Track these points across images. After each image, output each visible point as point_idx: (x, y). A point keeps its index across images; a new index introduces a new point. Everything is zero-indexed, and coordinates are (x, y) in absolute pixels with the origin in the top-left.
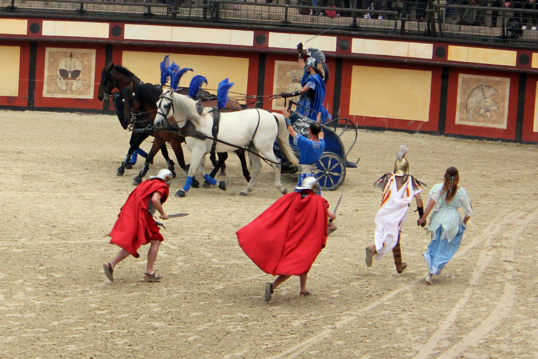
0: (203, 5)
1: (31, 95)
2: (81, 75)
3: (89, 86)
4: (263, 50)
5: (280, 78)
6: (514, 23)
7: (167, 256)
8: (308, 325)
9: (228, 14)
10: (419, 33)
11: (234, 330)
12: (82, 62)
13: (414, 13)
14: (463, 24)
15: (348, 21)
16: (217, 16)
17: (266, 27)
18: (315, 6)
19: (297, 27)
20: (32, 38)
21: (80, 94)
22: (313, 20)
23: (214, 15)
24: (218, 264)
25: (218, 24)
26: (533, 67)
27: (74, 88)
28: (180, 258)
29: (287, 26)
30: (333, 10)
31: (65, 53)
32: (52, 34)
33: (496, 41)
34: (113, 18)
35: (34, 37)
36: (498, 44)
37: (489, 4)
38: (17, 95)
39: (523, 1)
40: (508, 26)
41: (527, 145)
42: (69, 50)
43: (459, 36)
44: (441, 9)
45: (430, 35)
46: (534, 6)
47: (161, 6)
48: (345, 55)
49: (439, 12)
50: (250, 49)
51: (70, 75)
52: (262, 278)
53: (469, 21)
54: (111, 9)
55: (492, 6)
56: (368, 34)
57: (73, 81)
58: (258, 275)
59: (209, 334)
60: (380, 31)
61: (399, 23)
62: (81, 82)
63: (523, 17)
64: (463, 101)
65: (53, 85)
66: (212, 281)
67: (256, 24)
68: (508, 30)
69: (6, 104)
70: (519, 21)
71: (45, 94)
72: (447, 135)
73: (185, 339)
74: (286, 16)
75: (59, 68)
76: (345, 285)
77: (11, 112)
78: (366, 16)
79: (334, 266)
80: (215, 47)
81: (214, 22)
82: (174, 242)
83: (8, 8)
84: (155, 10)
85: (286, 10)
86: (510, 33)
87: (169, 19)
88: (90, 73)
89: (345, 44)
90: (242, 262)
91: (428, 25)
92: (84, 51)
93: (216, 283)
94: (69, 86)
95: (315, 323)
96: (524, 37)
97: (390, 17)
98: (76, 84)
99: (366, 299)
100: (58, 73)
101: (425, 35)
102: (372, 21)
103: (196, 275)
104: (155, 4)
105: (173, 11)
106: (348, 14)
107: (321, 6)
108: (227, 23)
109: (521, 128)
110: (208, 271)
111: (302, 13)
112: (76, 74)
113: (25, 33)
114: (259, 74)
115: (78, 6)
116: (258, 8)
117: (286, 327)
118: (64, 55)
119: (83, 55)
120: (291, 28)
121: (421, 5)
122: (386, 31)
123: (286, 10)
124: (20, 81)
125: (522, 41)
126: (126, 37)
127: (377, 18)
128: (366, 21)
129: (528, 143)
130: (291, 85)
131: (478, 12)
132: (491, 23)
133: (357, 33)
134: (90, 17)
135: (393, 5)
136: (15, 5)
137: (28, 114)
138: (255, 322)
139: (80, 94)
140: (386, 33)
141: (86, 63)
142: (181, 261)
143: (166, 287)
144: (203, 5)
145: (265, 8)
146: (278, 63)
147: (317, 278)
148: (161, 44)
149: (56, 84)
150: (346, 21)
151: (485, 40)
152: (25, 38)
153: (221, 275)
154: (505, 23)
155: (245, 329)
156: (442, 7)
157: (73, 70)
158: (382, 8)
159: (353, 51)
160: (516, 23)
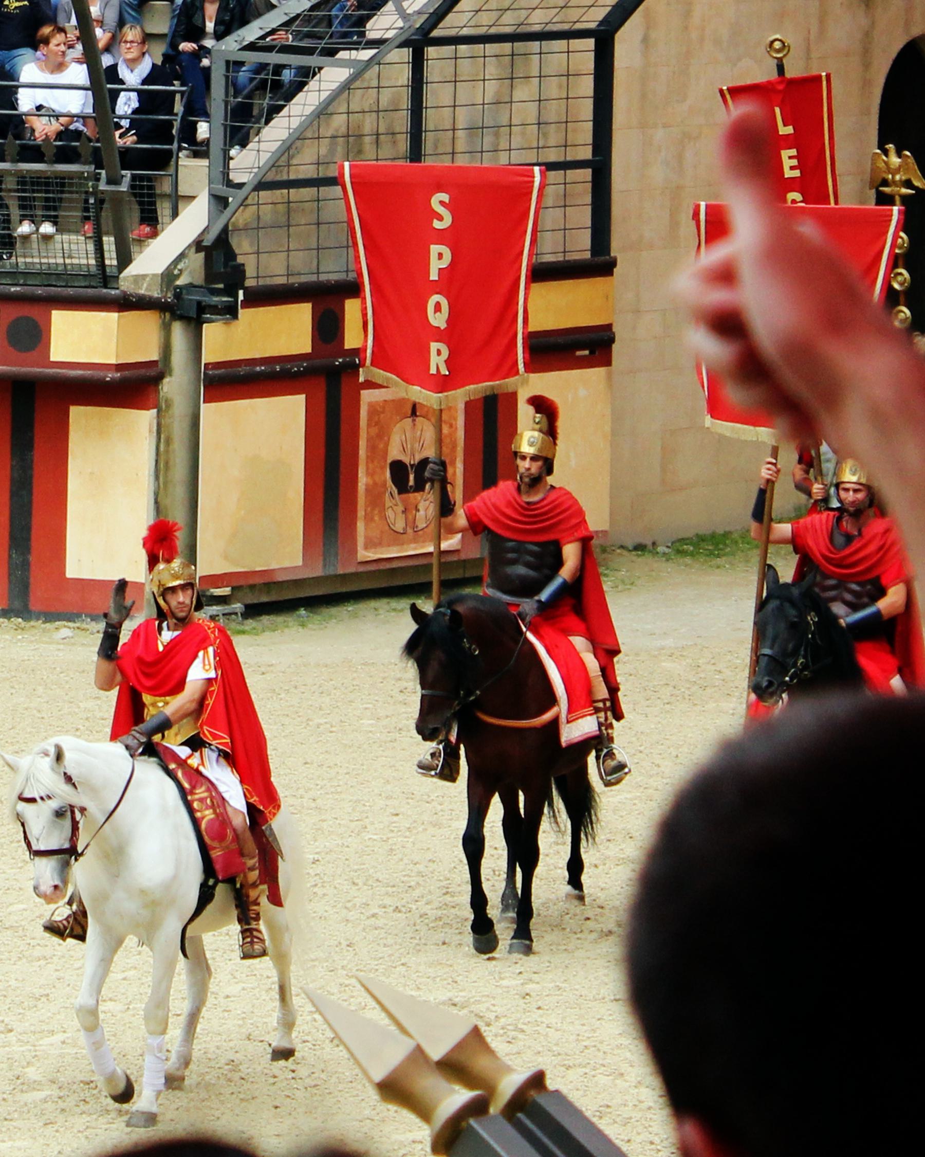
26: (53, 358)
39: (10, 137)
41: (48, 625)
46: (49, 153)
63: (17, 191)
96: (21, 260)
109: (25, 566)
125: (14, 275)
129: (50, 616)
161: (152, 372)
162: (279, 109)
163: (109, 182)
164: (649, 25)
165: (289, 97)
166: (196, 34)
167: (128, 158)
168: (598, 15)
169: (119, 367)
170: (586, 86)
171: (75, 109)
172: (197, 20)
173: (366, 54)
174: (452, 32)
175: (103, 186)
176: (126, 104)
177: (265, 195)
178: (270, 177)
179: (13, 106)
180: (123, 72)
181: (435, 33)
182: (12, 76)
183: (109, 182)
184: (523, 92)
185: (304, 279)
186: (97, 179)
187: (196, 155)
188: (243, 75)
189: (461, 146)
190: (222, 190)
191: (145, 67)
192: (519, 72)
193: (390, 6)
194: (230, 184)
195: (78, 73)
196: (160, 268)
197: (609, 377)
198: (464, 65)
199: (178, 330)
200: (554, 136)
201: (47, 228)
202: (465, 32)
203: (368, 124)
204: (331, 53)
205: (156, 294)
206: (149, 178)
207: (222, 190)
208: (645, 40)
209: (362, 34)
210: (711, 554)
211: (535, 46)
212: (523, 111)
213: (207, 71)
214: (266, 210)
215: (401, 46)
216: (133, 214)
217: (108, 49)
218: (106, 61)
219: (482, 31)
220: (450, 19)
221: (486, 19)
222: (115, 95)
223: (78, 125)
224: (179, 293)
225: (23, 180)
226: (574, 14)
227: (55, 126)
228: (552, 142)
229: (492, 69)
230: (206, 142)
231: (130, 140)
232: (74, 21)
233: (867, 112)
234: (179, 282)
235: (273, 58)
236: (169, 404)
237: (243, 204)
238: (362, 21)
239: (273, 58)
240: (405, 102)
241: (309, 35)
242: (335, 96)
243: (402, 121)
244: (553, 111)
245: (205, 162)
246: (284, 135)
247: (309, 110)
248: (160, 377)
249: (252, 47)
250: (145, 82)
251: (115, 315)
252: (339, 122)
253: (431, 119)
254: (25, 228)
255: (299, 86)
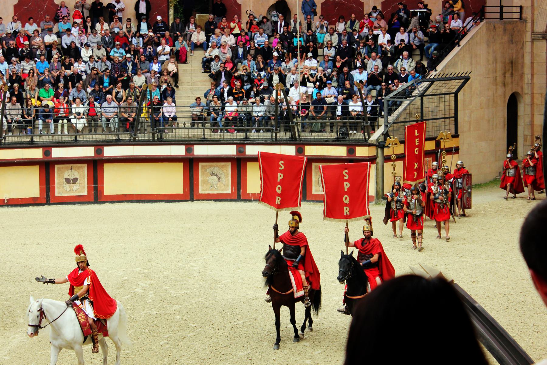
0: (152, 131)
1: (48, 196)
2: (78, 180)
3: (84, 187)
4: (191, 157)
5: (203, 174)
6: (344, 129)
7: (142, 291)
8: (234, 328)
9: (167, 136)
10: (286, 140)
11: (189, 335)
12: (79, 172)
13: (282, 128)
14: (313, 132)
15: (242, 135)
16: (161, 137)
17: (192, 142)
18: (221, 127)
19: (212, 141)
20: (46, 160)
21: (79, 192)
22: (221, 136)
23: (159, 137)
24: (175, 294)
25: (162, 142)
27: (75, 189)
28: (150, 292)
29: (205, 141)
30: (232, 129)
31: (67, 168)
32: (59, 156)
33: (333, 141)
34: (95, 144)
35: (47, 159)
36: (334, 143)
37: (327, 119)
38: (39, 196)
40: (340, 131)
42: (70, 166)
43: (311, 140)
44: (298, 124)
45: (293, 141)
47: (126, 134)
48: (242, 156)
49: (297, 126)
50: (183, 157)
51: (71, 181)
52: (203, 301)
53: (316, 130)
54: (94, 138)
55: (329, 120)
56: (255, 142)
57: (74, 185)
58: (200, 299)
59: (173, 339)
60: (262, 140)
61: (274, 134)
62: (78, 185)
64: (316, 179)
65: (61, 188)
66: (172, 305)
67: (185, 141)
68: (340, 134)
69: (32, 202)
70: (347, 128)
71: (57, 194)
72: (308, 201)
73: (158, 344)
74: (204, 135)
75: (65, 177)
76: (254, 301)
77: (36, 207)
78: (253, 131)
79: (246, 289)
80: (162, 157)
81: (159, 141)
82: (146, 282)
83: (29, 141)
84: (122, 137)
85: (204, 130)
86: (341, 136)
87: (131, 142)
88: (84, 179)
89: (242, 149)
90: (189, 291)
91: (292, 134)
92: (79, 165)
93: (174, 306)
94: (71, 188)
95: (238, 326)
97: (268, 131)
98: (76, 187)
99: (268, 308)
100: (64, 180)
101: (290, 141)
102: (256, 134)
103: (162, 302)
104: (122, 133)
105: (133, 136)
106: (243, 131)
107: (225, 127)
108: (168, 141)
110: (169, 299)
111: (213, 132)
112: (75, 180)
113: (41, 157)
114: (190, 172)
115: (74, 138)
116: (186, 131)
117: (220, 330)
118: (67, 168)
119: (79, 168)
120: (207, 142)
121: (287, 122)
122: (266, 140)
123: (204, 130)
124: (40, 187)
125: (349, 141)
126: (105, 155)
127: (259, 132)
128: (253, 135)
130: (210, 177)
131: (321, 124)
132: (329, 131)
133: (248, 142)
134: (81, 144)
135: (269, 124)
136: (34, 139)
137: (46, 207)
138: (201, 329)
139: (78, 193)
140: (266, 141)
141: (81, 173)
142: (151, 294)
143: (144, 311)
144: (152, 131)
145: (191, 131)
146: (201, 164)
147: (237, 298)
148: (127, 157)
149: (63, 187)
150: (242, 135)
151: (326, 141)
152: (41, 160)
153: (177, 301)
154: (338, 129)
155: (195, 334)
156: (299, 122)
157: (73, 178)
158: (262, 126)
159: (247, 154)
160: (344, 129)
161: (375, 157)
162: (397, 109)
163: (366, 123)
164: (464, 91)
165: (398, 107)
166: (381, 96)
167: (369, 119)
168: (455, 90)
169: (369, 157)
170: (453, 103)
171: (359, 110)
172: (381, 93)
173: (412, 98)
174: (428, 94)
175: (365, 124)
176: (369, 109)
177: (395, 125)
178: (395, 121)
179: (348, 110)
180: (368, 103)
181: (425, 94)
182: (348, 104)
183: (366, 123)
184: (441, 104)
185: (402, 140)
186: (364, 123)
187: (382, 118)
188: (390, 103)
189: (430, 114)
190: (387, 124)
191: (372, 102)
192: (441, 101)
193: (417, 89)
194: (388, 123)
195: (360, 103)
196: (376, 138)
197: (459, 157)
198: (431, 100)
199: (379, 150)
200: (447, 113)
201: (355, 132)
202: (431, 94)
203: (413, 111)
204: (406, 98)
205: (375, 143)
206: (373, 122)
207: (387, 124)
208: (464, 94)
209: (412, 95)
210: (478, 188)
211: (443, 96)
212: (442, 108)
213: (383, 102)
214: (395, 127)
215: (419, 96)
216: (371, 129)
217: (365, 99)
218: (365, 101)
219: (433, 93)
220: (428, 91)
221: (434, 91)
222: (367, 107)
223: (360, 113)
224: (379, 143)
225: (350, 123)
226: (450, 90)
227: (356, 113)
228: (447, 113)
229: (436, 101)
230: (384, 115)
231: (369, 115)
232: (359, 94)
233: (505, 106)
234: (379, 141)
235: (396, 100)
236: (378, 163)
237: (391, 126)
238: (412, 92)
239: (396, 100)
240: (420, 107)
241: (402, 95)
242: (407, 106)
243: (419, 110)
244: (447, 108)
245: (383, 119)
246: (398, 113)
247: (402, 109)
248: (376, 158)
249: (391, 98)
250: (372, 105)
251: (368, 147)
252: (408, 111)
253: (425, 110)
254: (351, 132)
255: (400, 105)
